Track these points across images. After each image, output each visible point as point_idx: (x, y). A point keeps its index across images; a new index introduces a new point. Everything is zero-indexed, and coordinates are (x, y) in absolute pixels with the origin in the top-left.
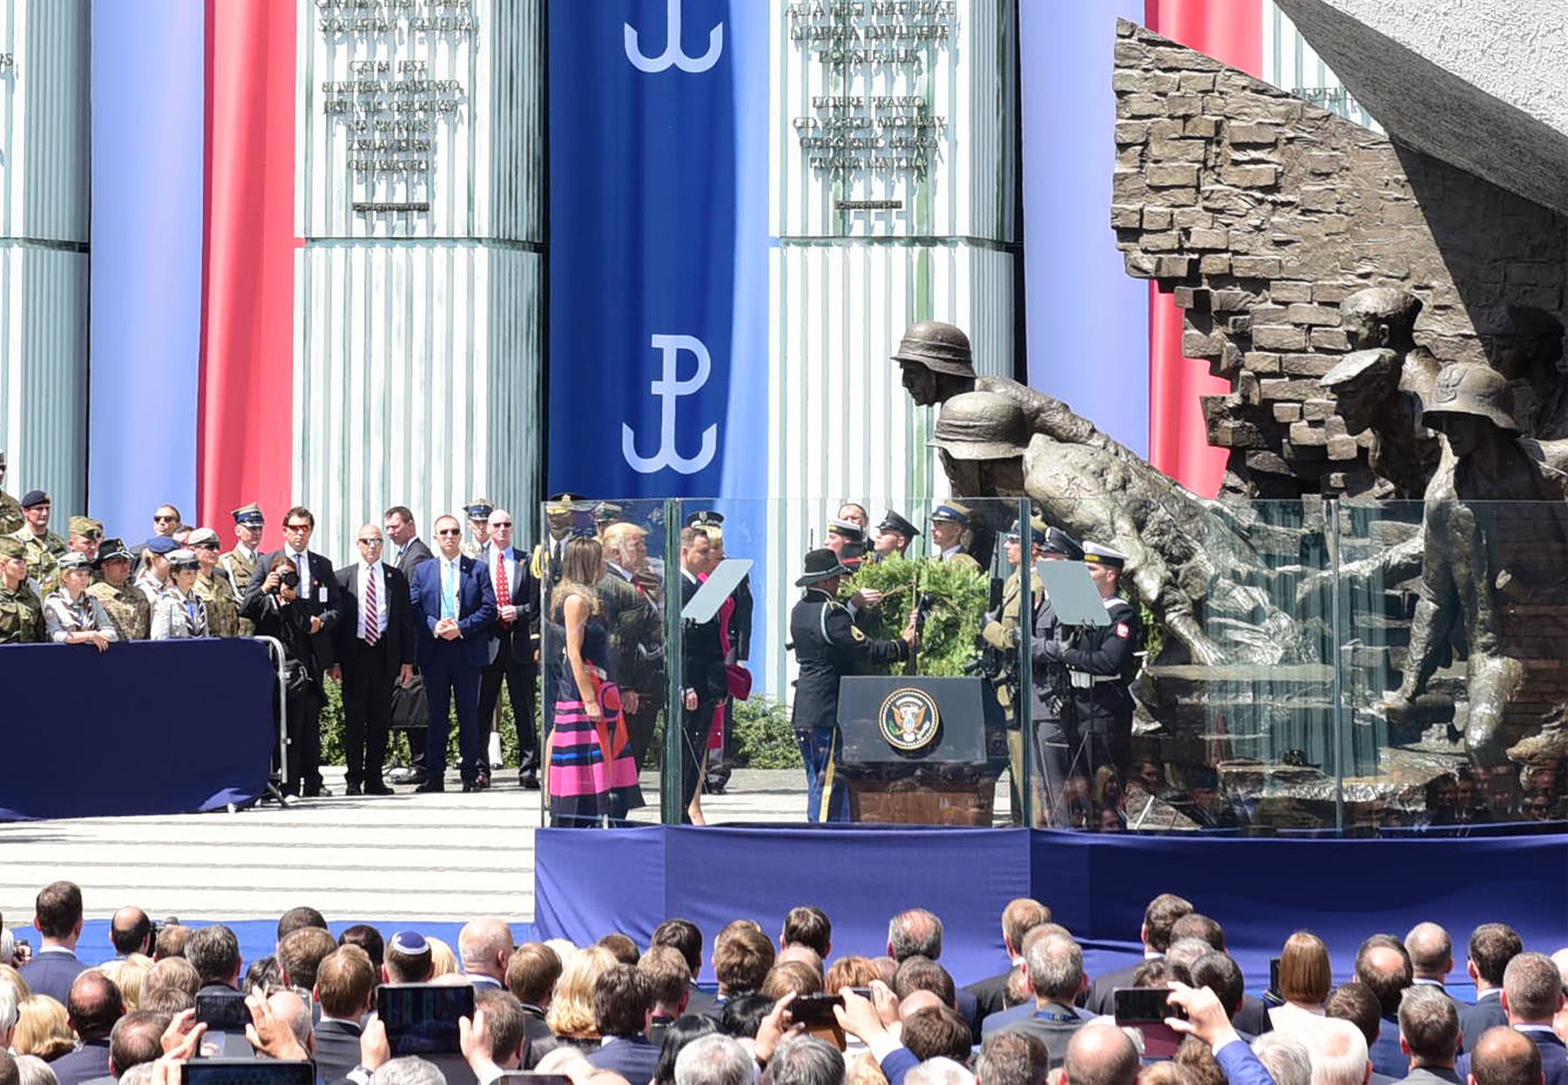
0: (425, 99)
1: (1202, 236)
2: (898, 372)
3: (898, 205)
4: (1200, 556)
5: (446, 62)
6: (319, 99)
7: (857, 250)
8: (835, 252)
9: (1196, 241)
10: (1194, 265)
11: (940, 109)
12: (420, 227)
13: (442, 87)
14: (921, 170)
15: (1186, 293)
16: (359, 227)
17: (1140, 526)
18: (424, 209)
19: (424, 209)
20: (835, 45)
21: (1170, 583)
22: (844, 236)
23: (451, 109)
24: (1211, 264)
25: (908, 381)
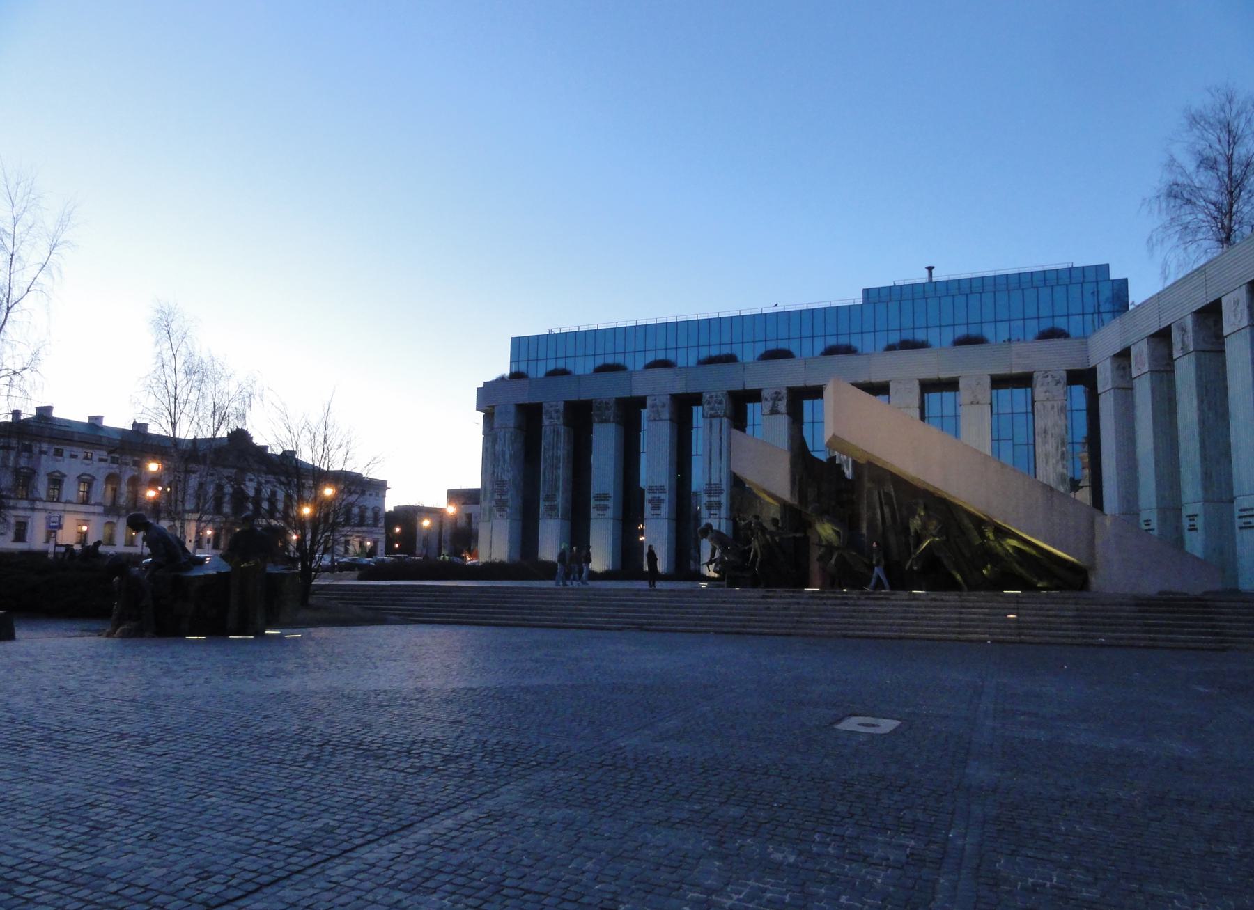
0: (660, 501)
5: (663, 496)
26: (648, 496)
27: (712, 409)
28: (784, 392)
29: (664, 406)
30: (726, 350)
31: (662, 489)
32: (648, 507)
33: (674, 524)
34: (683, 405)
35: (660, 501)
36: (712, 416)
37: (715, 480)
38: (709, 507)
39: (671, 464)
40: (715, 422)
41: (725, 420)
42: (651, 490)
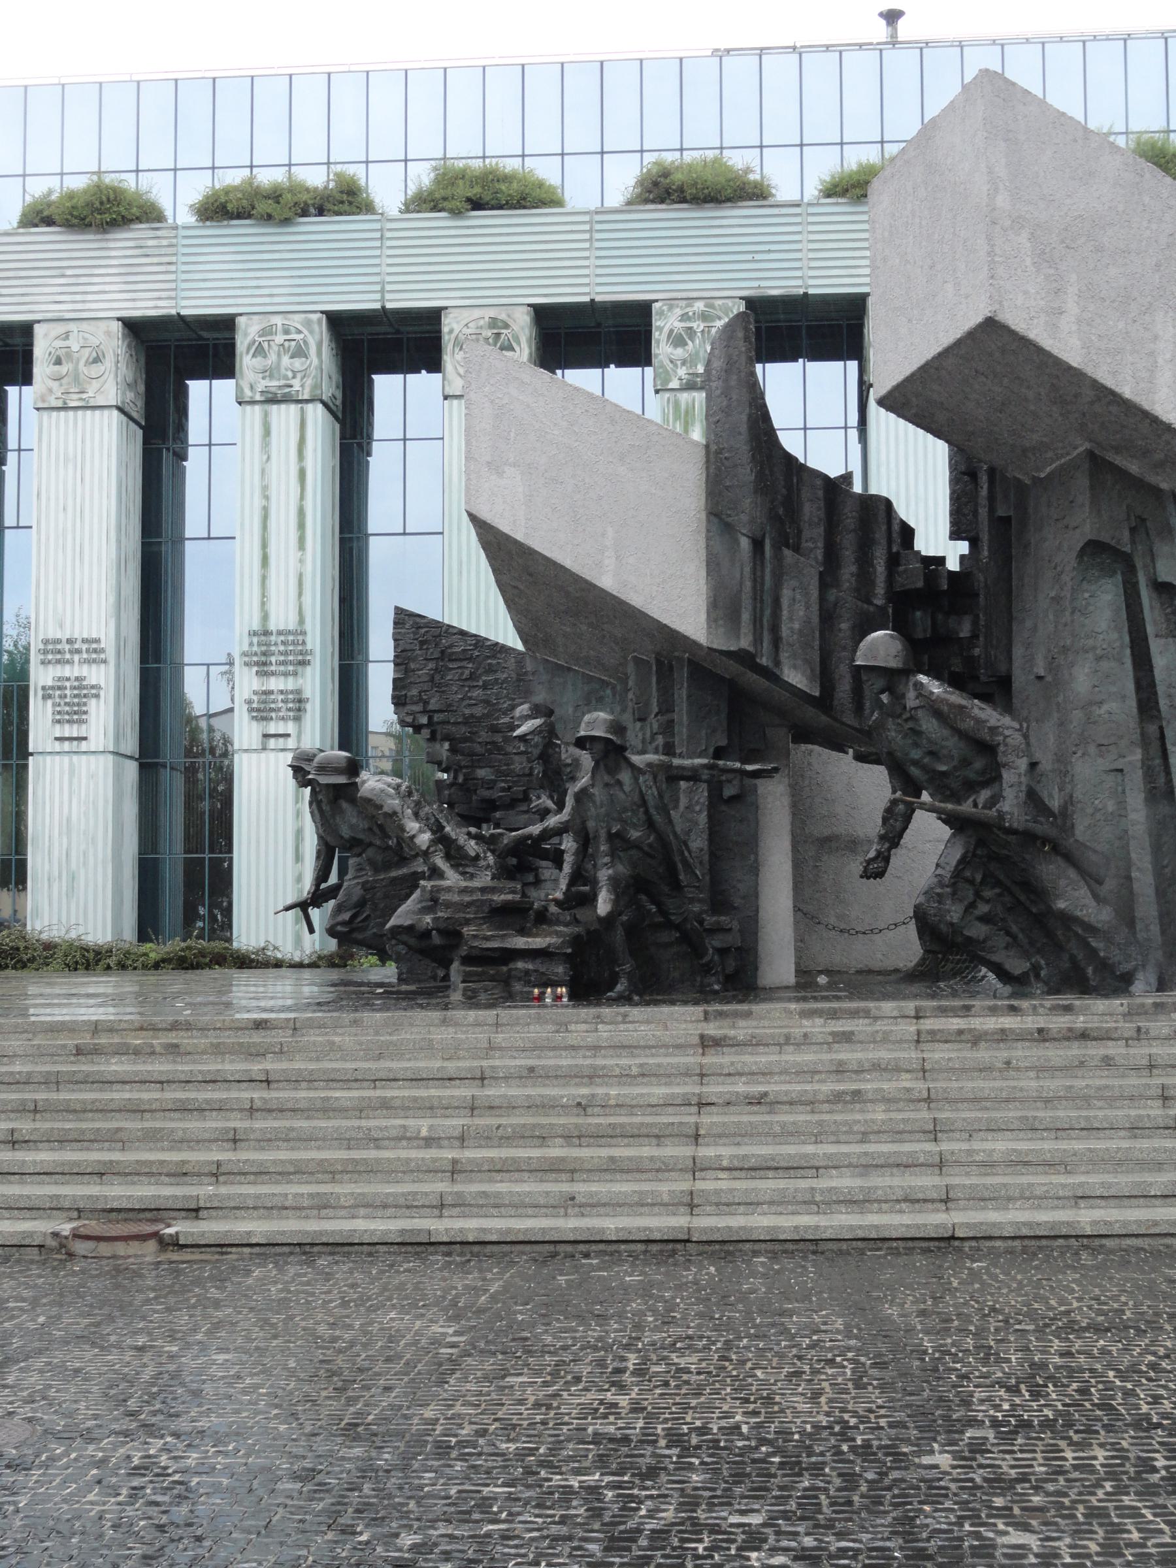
0: (84, 692)
1: (434, 704)
2: (290, 772)
3: (288, 735)
4: (448, 829)
6: (40, 693)
7: (272, 755)
8: (263, 755)
9: (431, 707)
10: (430, 718)
11: (307, 694)
12: (84, 746)
13: (93, 687)
14: (297, 719)
15: (426, 733)
16: (57, 746)
17: (416, 815)
18: (85, 739)
19: (85, 739)
20: (263, 668)
21: (433, 842)
22: (264, 749)
23: (97, 696)
24: (437, 718)
25: (295, 777)
26: (40, 676)
27: (268, 373)
28: (522, 325)
29: (97, 360)
30: (316, 178)
31: (92, 651)
32: (40, 716)
33: (131, 770)
34: (176, 355)
35: (84, 692)
36: (272, 399)
37: (282, 617)
38: (262, 711)
39: (120, 565)
40: (285, 416)
41: (317, 414)
42: (55, 652)
